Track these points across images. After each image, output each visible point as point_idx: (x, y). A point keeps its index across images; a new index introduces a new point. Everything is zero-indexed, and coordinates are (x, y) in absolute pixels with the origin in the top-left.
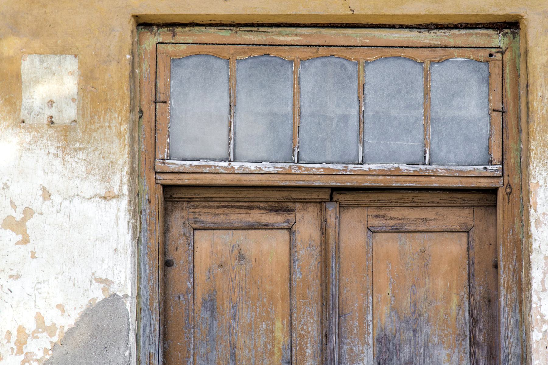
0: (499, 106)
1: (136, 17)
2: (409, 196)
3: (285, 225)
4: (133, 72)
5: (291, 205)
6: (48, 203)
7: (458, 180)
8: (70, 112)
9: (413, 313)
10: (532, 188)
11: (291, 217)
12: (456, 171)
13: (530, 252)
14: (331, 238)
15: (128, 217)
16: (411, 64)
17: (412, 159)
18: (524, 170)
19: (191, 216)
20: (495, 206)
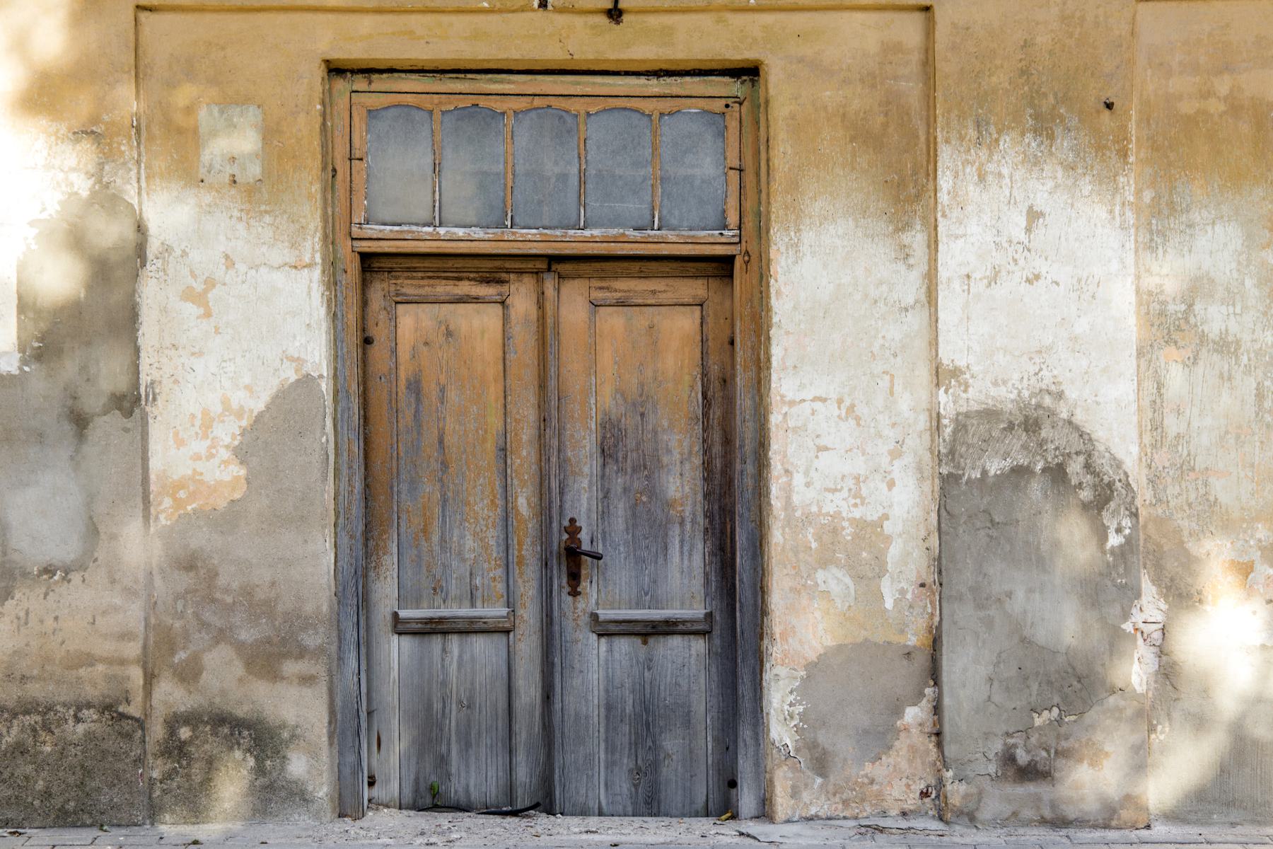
0: (736, 164)
1: (327, 62)
2: (636, 266)
3: (498, 298)
4: (324, 124)
5: (504, 276)
6: (232, 272)
7: (690, 246)
8: (255, 170)
9: (641, 396)
10: (772, 256)
11: (505, 288)
12: (689, 237)
13: (769, 327)
14: (549, 312)
15: (322, 289)
16: (638, 116)
17: (640, 223)
18: (763, 235)
19: (392, 288)
20: (731, 276)
